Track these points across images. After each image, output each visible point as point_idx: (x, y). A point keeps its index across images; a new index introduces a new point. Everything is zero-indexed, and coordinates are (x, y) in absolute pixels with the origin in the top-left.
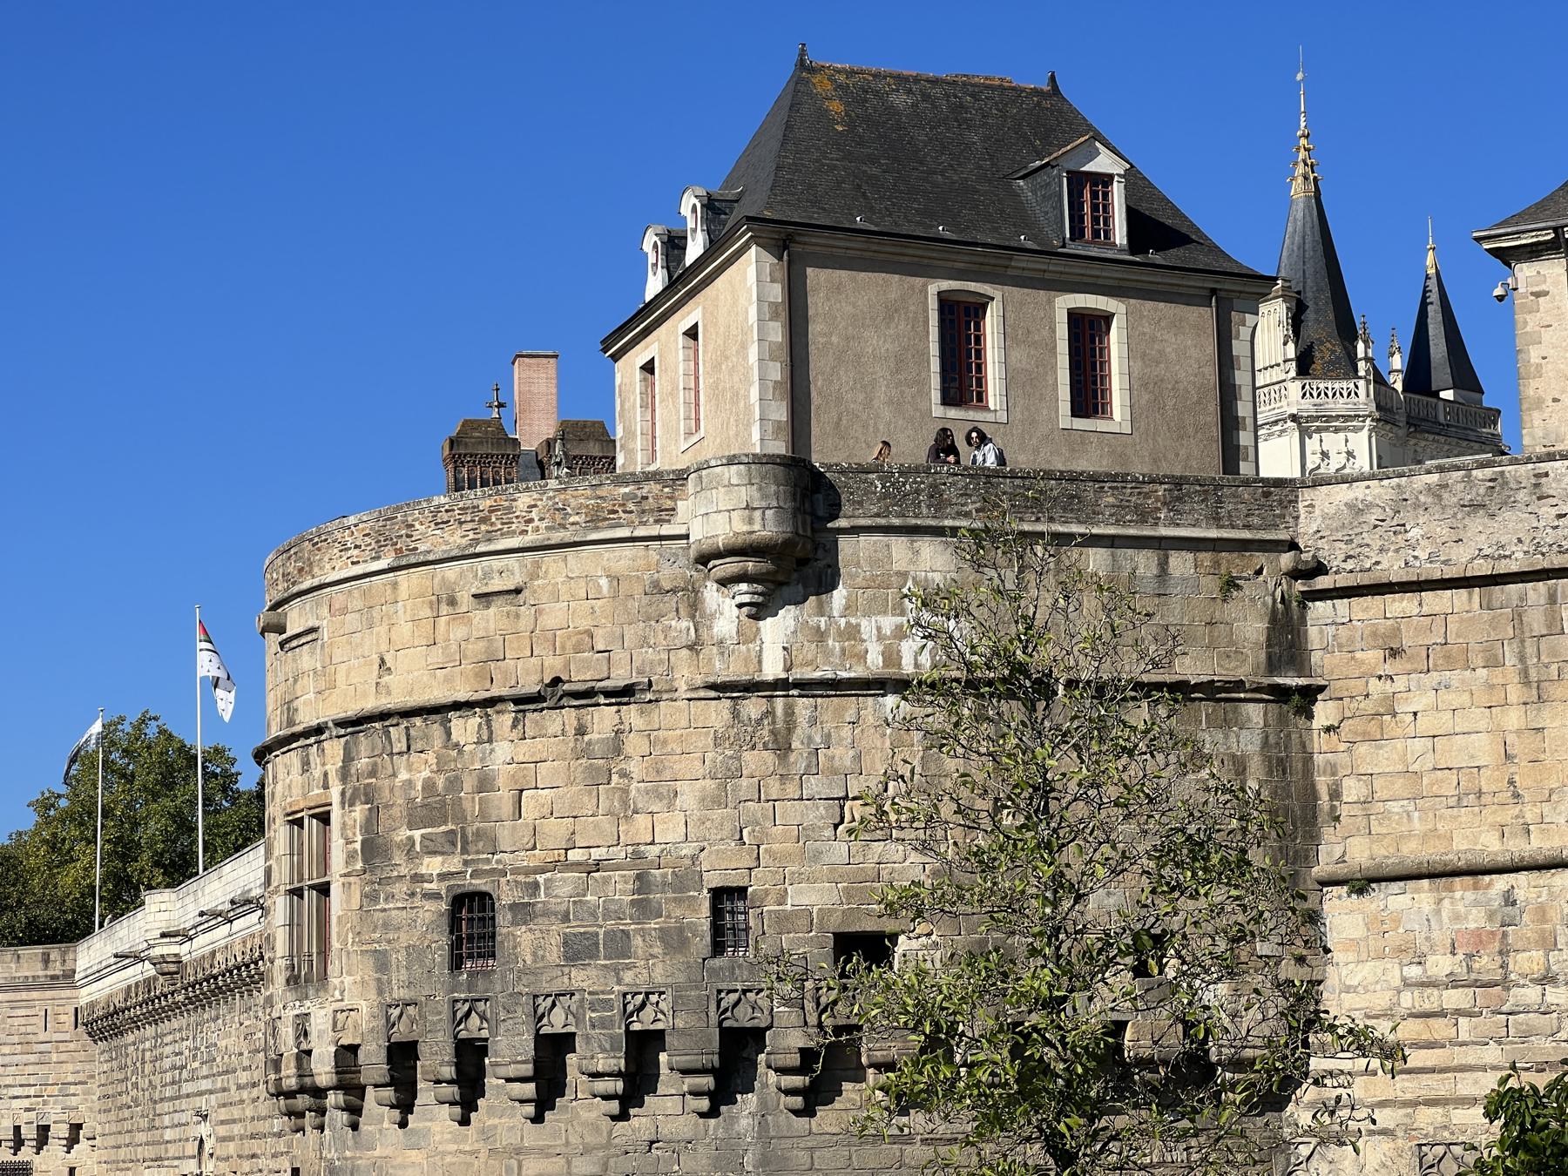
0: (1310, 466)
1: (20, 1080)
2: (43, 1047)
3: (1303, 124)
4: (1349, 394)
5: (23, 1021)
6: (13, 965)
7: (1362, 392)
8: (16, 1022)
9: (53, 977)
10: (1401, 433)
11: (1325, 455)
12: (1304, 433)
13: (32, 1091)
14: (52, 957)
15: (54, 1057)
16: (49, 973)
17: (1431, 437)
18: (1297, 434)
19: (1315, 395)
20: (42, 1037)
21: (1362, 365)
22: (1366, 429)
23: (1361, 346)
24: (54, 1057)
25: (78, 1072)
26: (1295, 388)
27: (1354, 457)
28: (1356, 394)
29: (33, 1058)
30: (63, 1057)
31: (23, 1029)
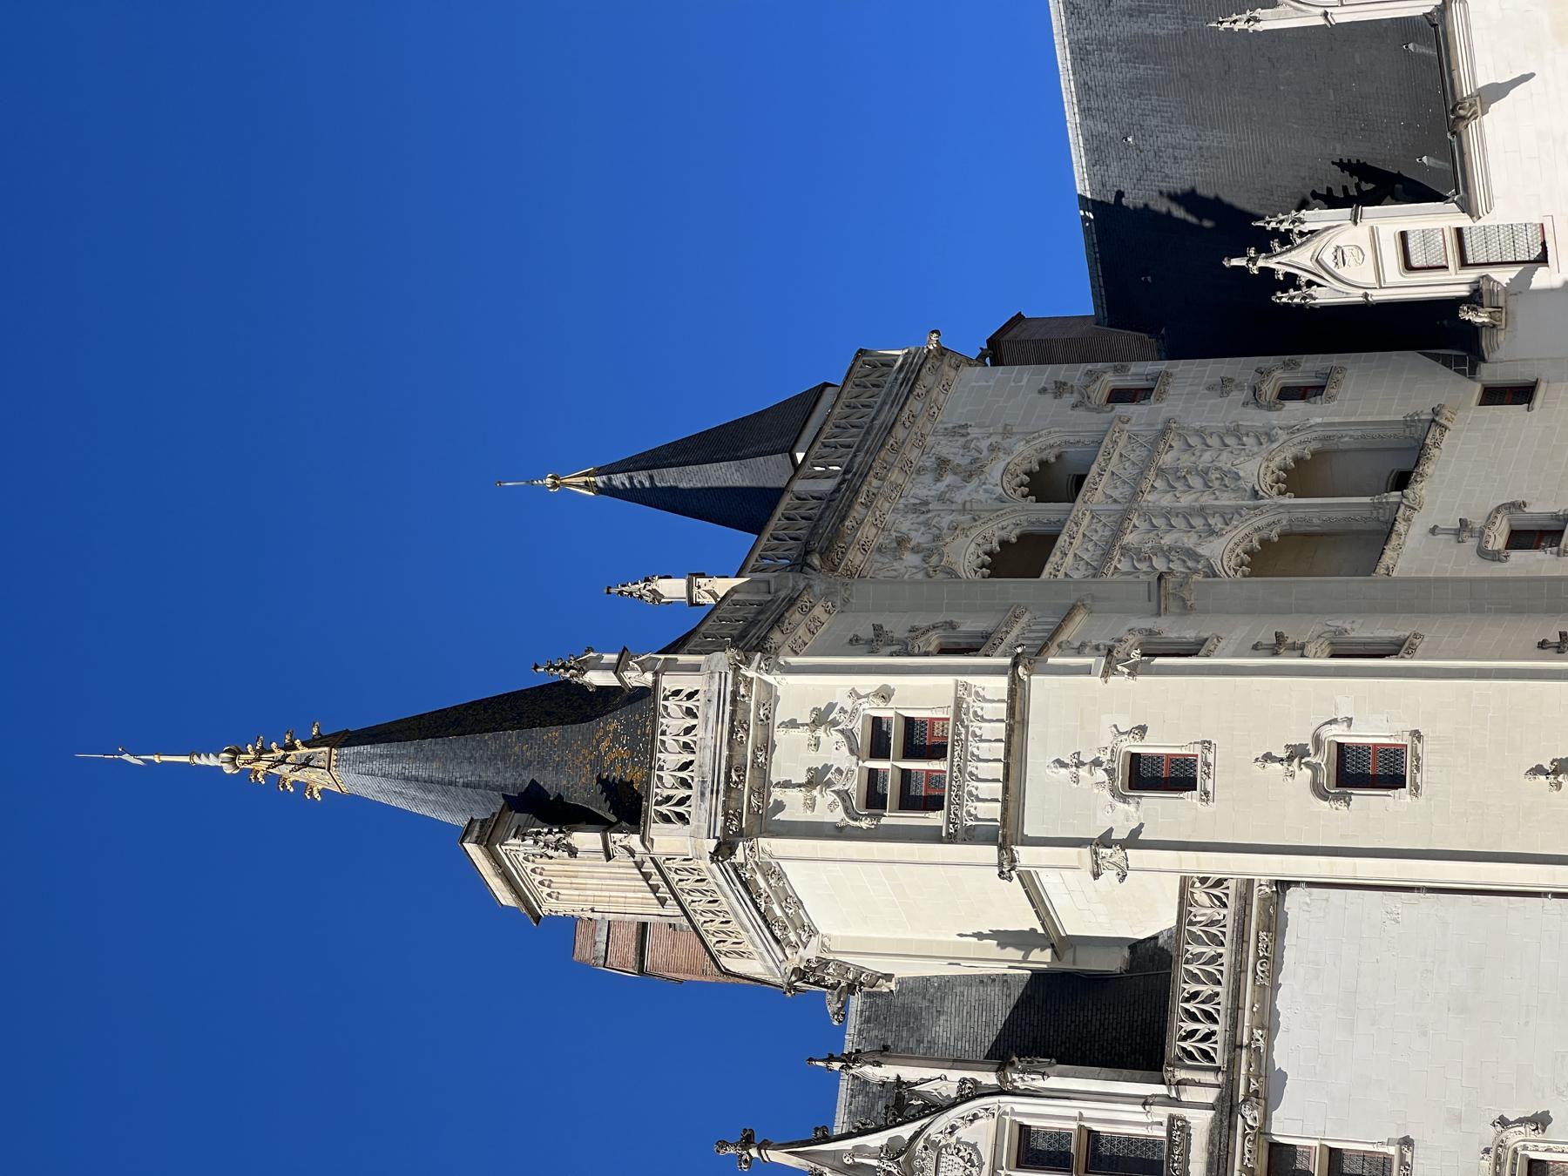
0: (838, 816)
3: (212, 761)
4: (690, 713)
7: (686, 682)
10: (818, 587)
11: (817, 779)
12: (768, 824)
17: (858, 511)
18: (763, 842)
19: (683, 792)
21: (636, 678)
22: (766, 677)
23: (597, 678)
26: (667, 840)
27: (831, 706)
28: (690, 696)
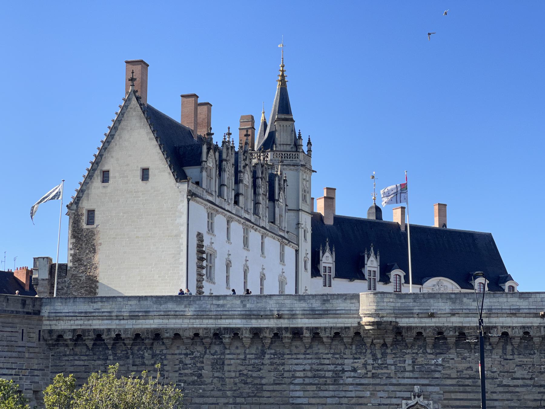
1: (9, 366)
2: (20, 349)
5: (9, 334)
6: (5, 304)
8: (5, 334)
9: (28, 313)
13: (13, 372)
14: (27, 302)
15: (27, 355)
16: (25, 310)
20: (20, 343)
24: (27, 355)
25: (39, 364)
29: (14, 354)
30: (32, 355)
31: (9, 339)
